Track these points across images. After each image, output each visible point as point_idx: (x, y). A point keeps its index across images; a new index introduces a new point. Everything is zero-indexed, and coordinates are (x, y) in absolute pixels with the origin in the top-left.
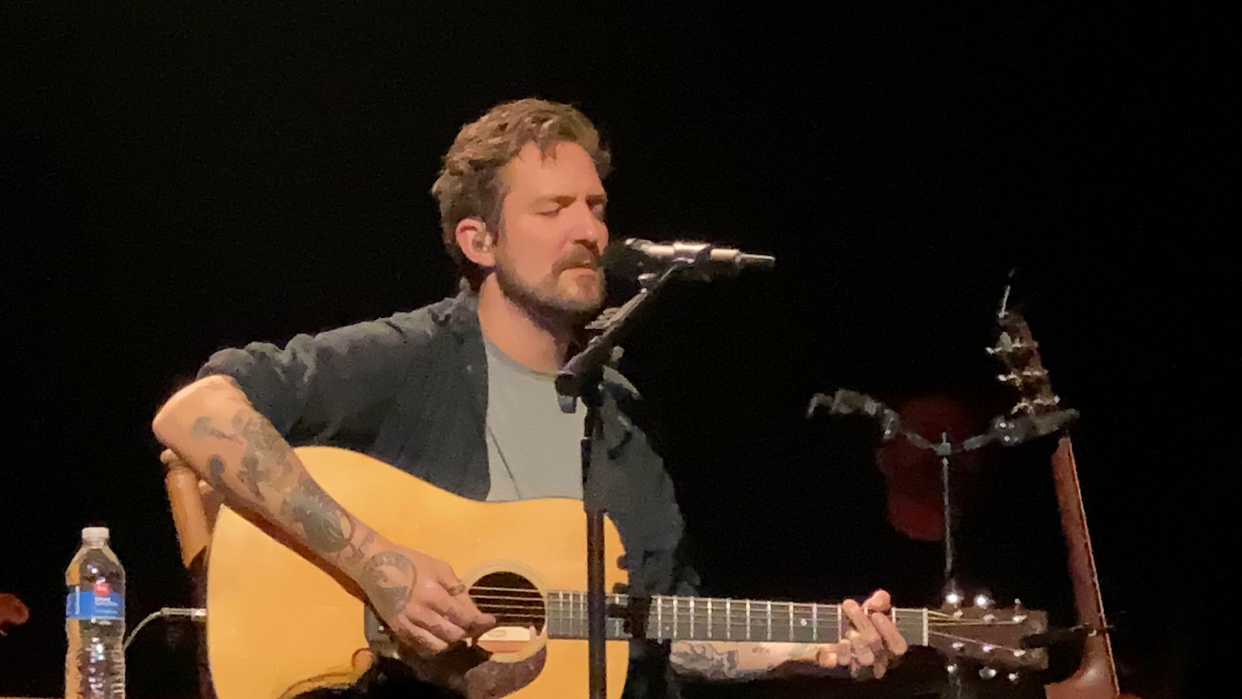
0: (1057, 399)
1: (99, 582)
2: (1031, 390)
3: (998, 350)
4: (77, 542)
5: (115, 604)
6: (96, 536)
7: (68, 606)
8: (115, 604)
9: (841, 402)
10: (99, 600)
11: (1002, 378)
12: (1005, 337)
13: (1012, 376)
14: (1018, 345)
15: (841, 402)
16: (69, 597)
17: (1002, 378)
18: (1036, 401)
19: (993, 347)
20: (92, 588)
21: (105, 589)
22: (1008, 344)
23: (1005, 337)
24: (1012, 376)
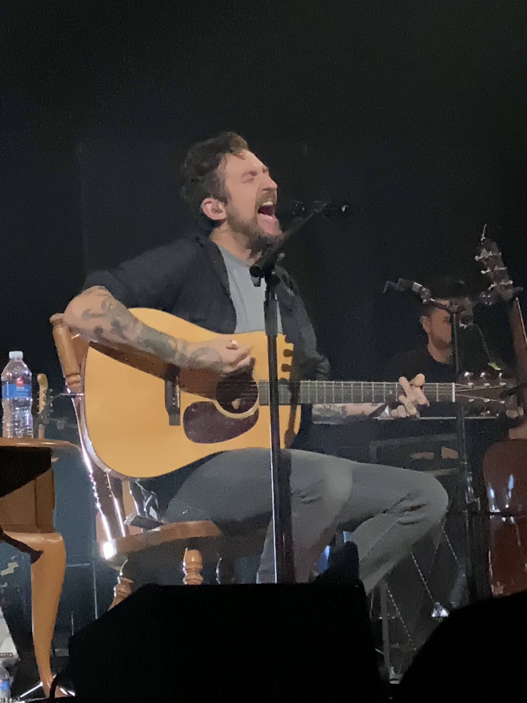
0: (511, 282)
1: (18, 379)
2: (498, 277)
3: (480, 258)
4: (7, 359)
5: (27, 390)
6: (16, 355)
7: (3, 392)
8: (27, 390)
9: (399, 285)
10: (18, 388)
11: (483, 272)
12: (484, 251)
13: (488, 271)
14: (491, 254)
15: (399, 285)
16: (3, 387)
17: (483, 272)
18: (501, 284)
19: (479, 256)
20: (16, 382)
21: (21, 382)
22: (485, 254)
23: (484, 251)
24: (488, 271)
